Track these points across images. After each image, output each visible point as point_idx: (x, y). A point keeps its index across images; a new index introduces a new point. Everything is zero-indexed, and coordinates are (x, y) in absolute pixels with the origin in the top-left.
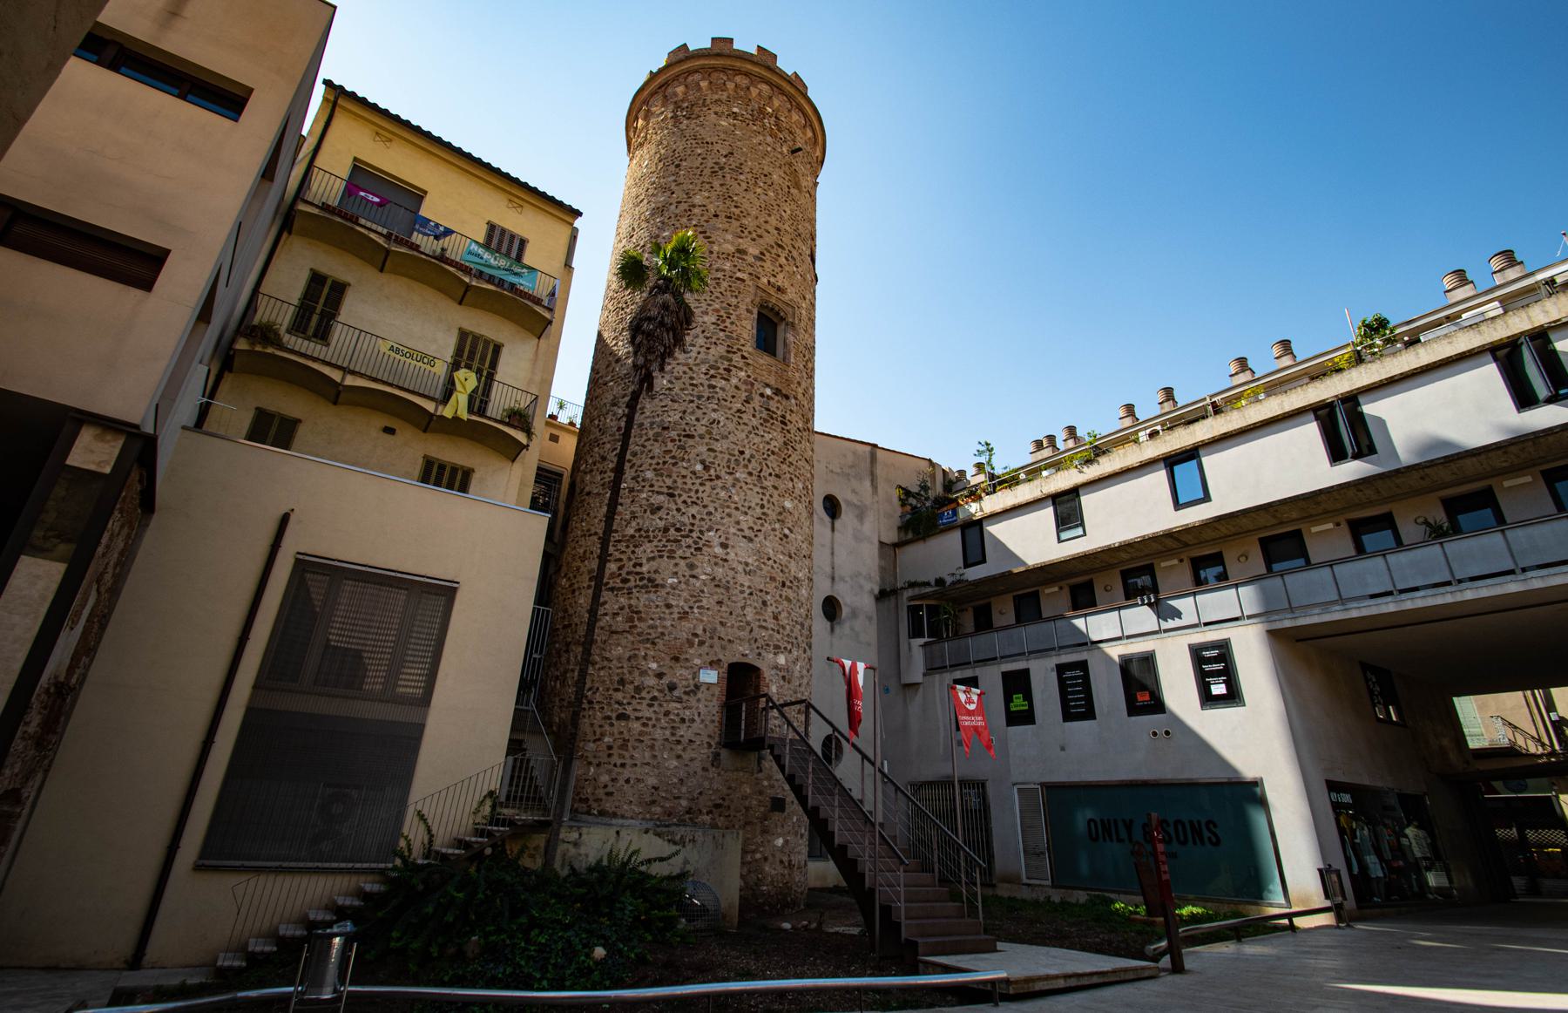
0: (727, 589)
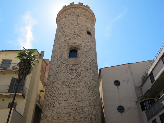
0: (60, 114)
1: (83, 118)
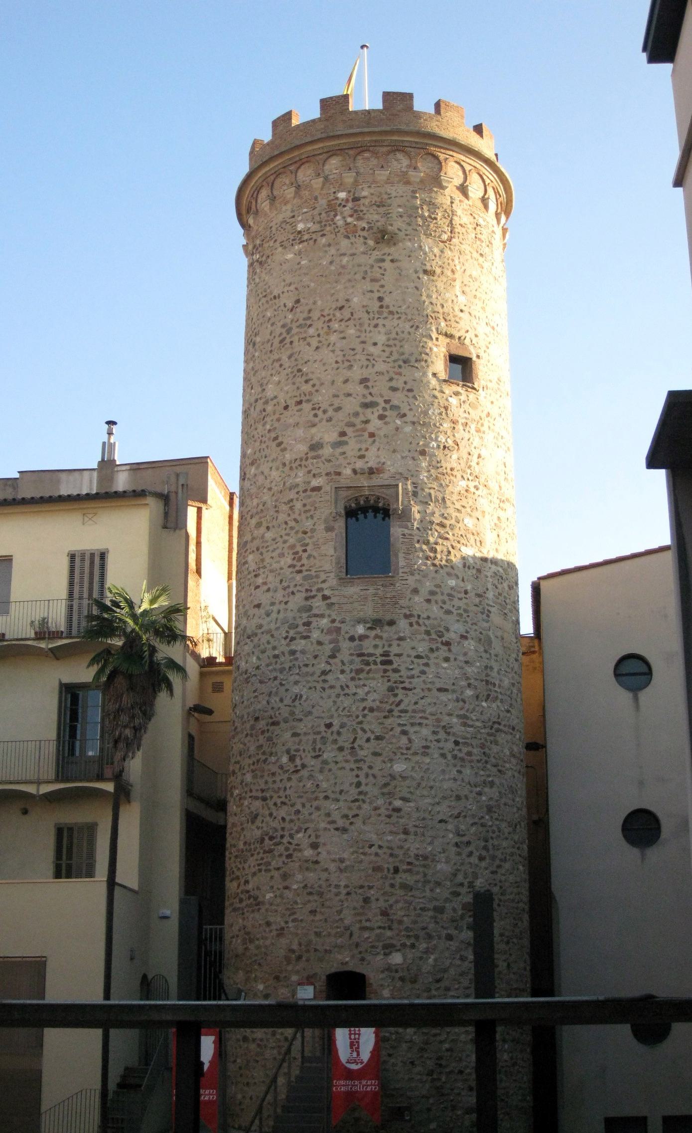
1: (429, 910)
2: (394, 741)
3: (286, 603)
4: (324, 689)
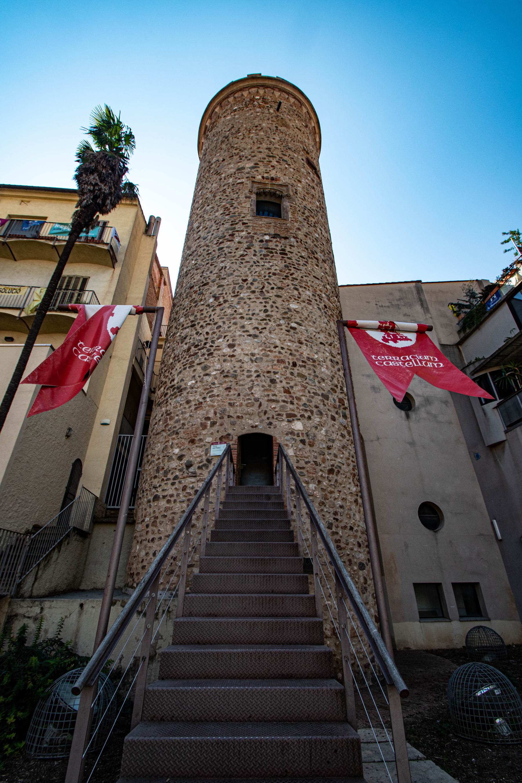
0: (235, 377)
2: (290, 291)
3: (218, 229)
4: (242, 263)
